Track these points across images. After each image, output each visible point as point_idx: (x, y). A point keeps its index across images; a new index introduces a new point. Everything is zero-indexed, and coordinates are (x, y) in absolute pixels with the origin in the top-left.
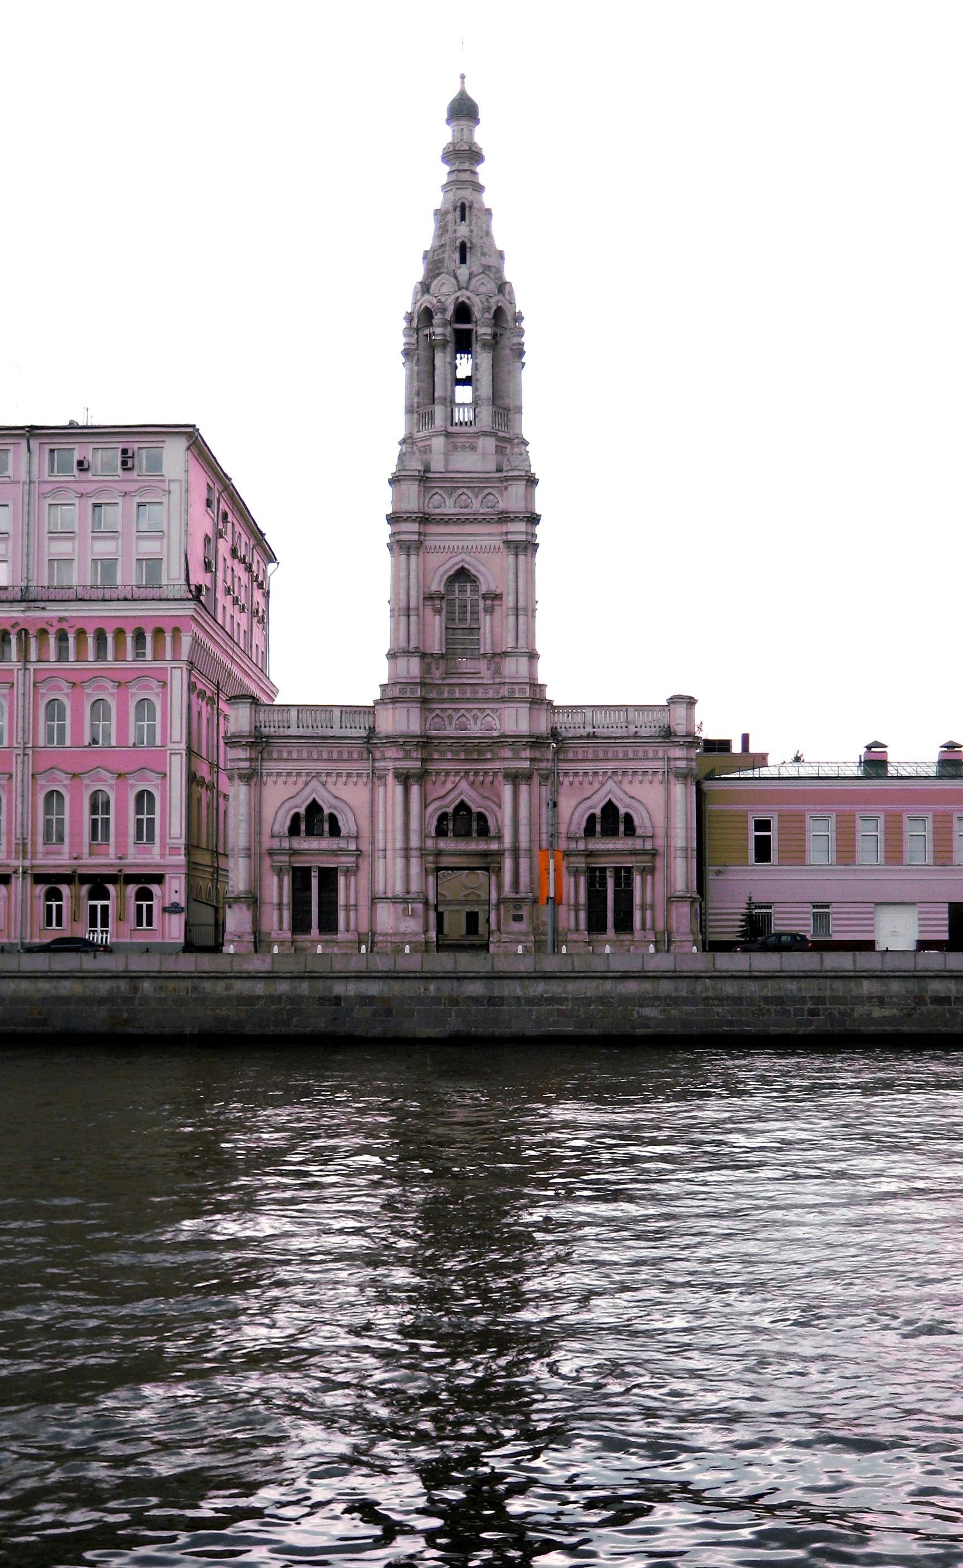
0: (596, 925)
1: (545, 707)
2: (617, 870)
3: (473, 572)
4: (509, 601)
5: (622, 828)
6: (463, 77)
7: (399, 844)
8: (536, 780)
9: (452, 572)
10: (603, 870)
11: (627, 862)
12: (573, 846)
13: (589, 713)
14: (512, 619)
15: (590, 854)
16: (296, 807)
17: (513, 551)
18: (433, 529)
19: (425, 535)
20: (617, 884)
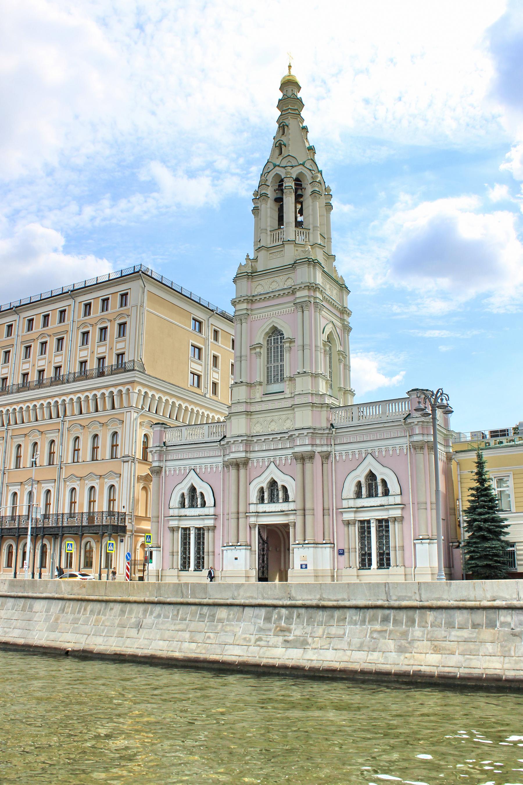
0: (365, 562)
1: (325, 409)
2: (380, 521)
3: (279, 328)
4: (299, 342)
5: (380, 490)
6: (290, 67)
7: (233, 509)
8: (318, 459)
9: (267, 330)
10: (369, 522)
11: (382, 515)
12: (345, 504)
13: (355, 409)
14: (300, 352)
15: (358, 509)
16: (182, 488)
17: (300, 310)
18: (256, 306)
19: (252, 310)
20: (378, 531)
